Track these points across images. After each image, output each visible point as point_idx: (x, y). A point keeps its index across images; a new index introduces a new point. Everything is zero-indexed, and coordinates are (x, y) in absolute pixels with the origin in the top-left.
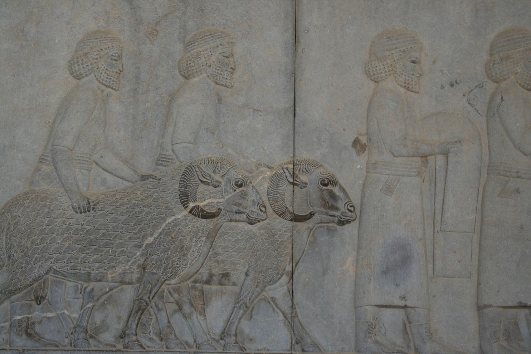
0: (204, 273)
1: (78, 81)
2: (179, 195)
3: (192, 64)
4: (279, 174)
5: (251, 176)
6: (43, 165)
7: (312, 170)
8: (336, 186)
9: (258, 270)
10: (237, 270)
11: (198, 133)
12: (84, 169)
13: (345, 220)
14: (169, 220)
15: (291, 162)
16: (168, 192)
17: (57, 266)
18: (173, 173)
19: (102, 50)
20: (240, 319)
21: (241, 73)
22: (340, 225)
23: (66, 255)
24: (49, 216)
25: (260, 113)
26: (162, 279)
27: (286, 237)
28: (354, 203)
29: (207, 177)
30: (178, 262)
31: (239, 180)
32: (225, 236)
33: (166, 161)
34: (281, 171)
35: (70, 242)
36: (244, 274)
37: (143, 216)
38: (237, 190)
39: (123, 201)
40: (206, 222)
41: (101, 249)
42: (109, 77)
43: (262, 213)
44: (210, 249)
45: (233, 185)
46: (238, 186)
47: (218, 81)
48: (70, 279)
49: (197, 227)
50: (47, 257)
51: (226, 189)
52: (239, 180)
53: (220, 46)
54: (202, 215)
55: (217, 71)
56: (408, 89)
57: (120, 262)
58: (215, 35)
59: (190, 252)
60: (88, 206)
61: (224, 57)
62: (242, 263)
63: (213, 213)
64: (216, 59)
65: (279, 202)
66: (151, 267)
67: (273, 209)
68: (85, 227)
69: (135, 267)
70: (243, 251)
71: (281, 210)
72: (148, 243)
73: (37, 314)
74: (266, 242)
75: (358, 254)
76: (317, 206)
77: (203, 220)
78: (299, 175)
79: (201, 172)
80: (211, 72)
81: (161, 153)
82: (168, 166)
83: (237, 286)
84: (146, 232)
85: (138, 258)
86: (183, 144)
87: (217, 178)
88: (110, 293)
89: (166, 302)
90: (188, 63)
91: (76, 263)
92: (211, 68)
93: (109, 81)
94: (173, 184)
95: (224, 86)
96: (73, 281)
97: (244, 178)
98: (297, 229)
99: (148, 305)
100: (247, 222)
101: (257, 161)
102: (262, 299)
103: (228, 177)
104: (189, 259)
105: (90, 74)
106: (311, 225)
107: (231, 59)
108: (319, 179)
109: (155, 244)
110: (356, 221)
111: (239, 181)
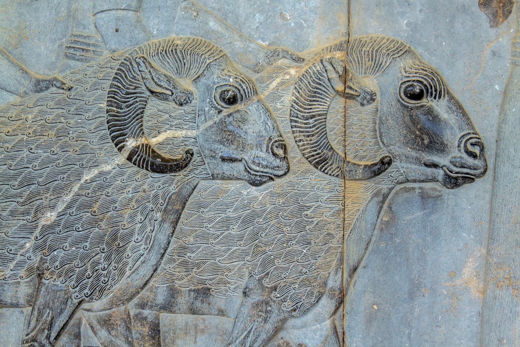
0: (158, 287)
2: (108, 123)
4: (314, 73)
5: (257, 80)
7: (386, 62)
8: (440, 97)
9: (269, 286)
10: (226, 283)
13: (459, 175)
14: (87, 177)
15: (341, 45)
16: (87, 115)
18: (96, 75)
26: (74, 299)
28: (481, 135)
29: (162, 84)
30: (104, 264)
31: (229, 88)
32: (202, 209)
33: (83, 50)
34: (318, 68)
36: (240, 292)
37: (37, 168)
38: (225, 110)
43: (278, 161)
44: (172, 236)
45: (215, 100)
46: (225, 102)
49: (144, 191)
51: (202, 110)
54: (153, 164)
59: (130, 244)
62: (236, 270)
63: (176, 160)
65: (313, 135)
66: (52, 273)
67: (301, 150)
70: (238, 243)
71: (318, 154)
74: (285, 225)
75: (488, 251)
76: (398, 145)
77: (156, 175)
79: (150, 72)
81: (75, 33)
82: (86, 60)
84: (41, 201)
94: (95, 100)
97: (240, 85)
104: (128, 257)
106: (385, 187)
108: (402, 84)
110: (486, 177)
111: (228, 91)
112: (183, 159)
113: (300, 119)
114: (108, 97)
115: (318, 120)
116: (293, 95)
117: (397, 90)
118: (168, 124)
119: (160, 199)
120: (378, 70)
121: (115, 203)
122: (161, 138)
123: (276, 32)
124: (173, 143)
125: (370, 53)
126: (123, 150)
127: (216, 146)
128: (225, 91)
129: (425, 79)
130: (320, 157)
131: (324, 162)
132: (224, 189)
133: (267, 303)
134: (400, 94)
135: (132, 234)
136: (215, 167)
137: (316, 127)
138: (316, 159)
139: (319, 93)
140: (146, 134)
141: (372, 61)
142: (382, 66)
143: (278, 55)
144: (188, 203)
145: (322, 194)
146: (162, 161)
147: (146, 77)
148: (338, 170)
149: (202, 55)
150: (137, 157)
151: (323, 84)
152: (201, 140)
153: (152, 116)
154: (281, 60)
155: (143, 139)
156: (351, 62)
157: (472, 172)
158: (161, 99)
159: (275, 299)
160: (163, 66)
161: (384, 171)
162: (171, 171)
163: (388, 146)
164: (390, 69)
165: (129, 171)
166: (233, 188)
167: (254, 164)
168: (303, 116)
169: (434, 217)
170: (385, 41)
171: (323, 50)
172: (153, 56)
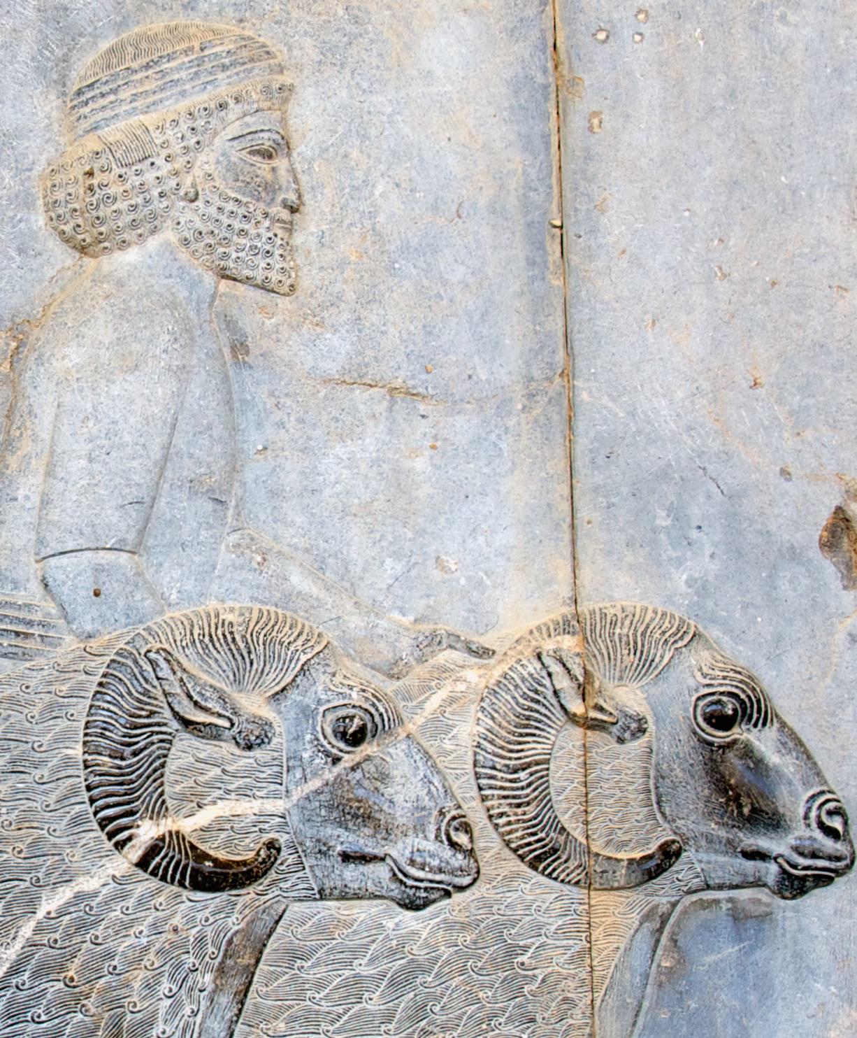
2: (89, 788)
3: (114, 189)
4: (523, 680)
5: (396, 692)
7: (662, 657)
8: (764, 724)
11: (154, 499)
15: (566, 622)
21: (324, 227)
22: (787, 894)
25: (422, 408)
29: (209, 705)
31: (352, 711)
38: (346, 757)
43: (460, 856)
45: (325, 737)
46: (347, 742)
49: (175, 930)
53: (231, 102)
54: (195, 872)
55: (226, 221)
61: (250, 153)
63: (244, 863)
64: (218, 162)
65: (528, 804)
67: (502, 835)
76: (692, 818)
77: (199, 895)
79: (181, 680)
80: (199, 225)
86: (89, 554)
87: (253, 704)
90: (95, 181)
92: (199, 203)
95: (257, 286)
97: (373, 705)
100: (393, 899)
103: (299, 698)
106: (664, 900)
107: (281, 163)
108: (698, 699)
111: (352, 718)
112: (260, 859)
113: (500, 771)
114: (86, 735)
115: (536, 772)
116: (478, 724)
117: (688, 712)
118: (220, 788)
119: (209, 945)
120: (647, 671)
121: (112, 958)
122: (204, 817)
123: (428, 596)
124: (232, 827)
125: (631, 638)
126: (129, 845)
127: (329, 831)
128: (344, 718)
129: (744, 691)
130: (544, 846)
131: (551, 855)
132: (344, 918)
134: (695, 718)
136: (326, 873)
137: (533, 787)
139: (536, 720)
140: (171, 812)
141: (635, 654)
142: (654, 665)
143: (440, 642)
144: (267, 951)
145: (545, 920)
146: (215, 866)
147: (173, 691)
148: (578, 871)
149: (289, 643)
150: (163, 859)
151: (542, 700)
152: (294, 820)
153: (184, 772)
154: (444, 653)
155: (170, 820)
156: (595, 656)
158: (203, 737)
160: (205, 667)
161: (665, 870)
162: (234, 887)
163: (674, 821)
164: (671, 669)
165: (139, 890)
166: (363, 916)
167: (413, 866)
168: (507, 766)
169: (759, 955)
170: (650, 615)
171: (531, 632)
172: (183, 648)
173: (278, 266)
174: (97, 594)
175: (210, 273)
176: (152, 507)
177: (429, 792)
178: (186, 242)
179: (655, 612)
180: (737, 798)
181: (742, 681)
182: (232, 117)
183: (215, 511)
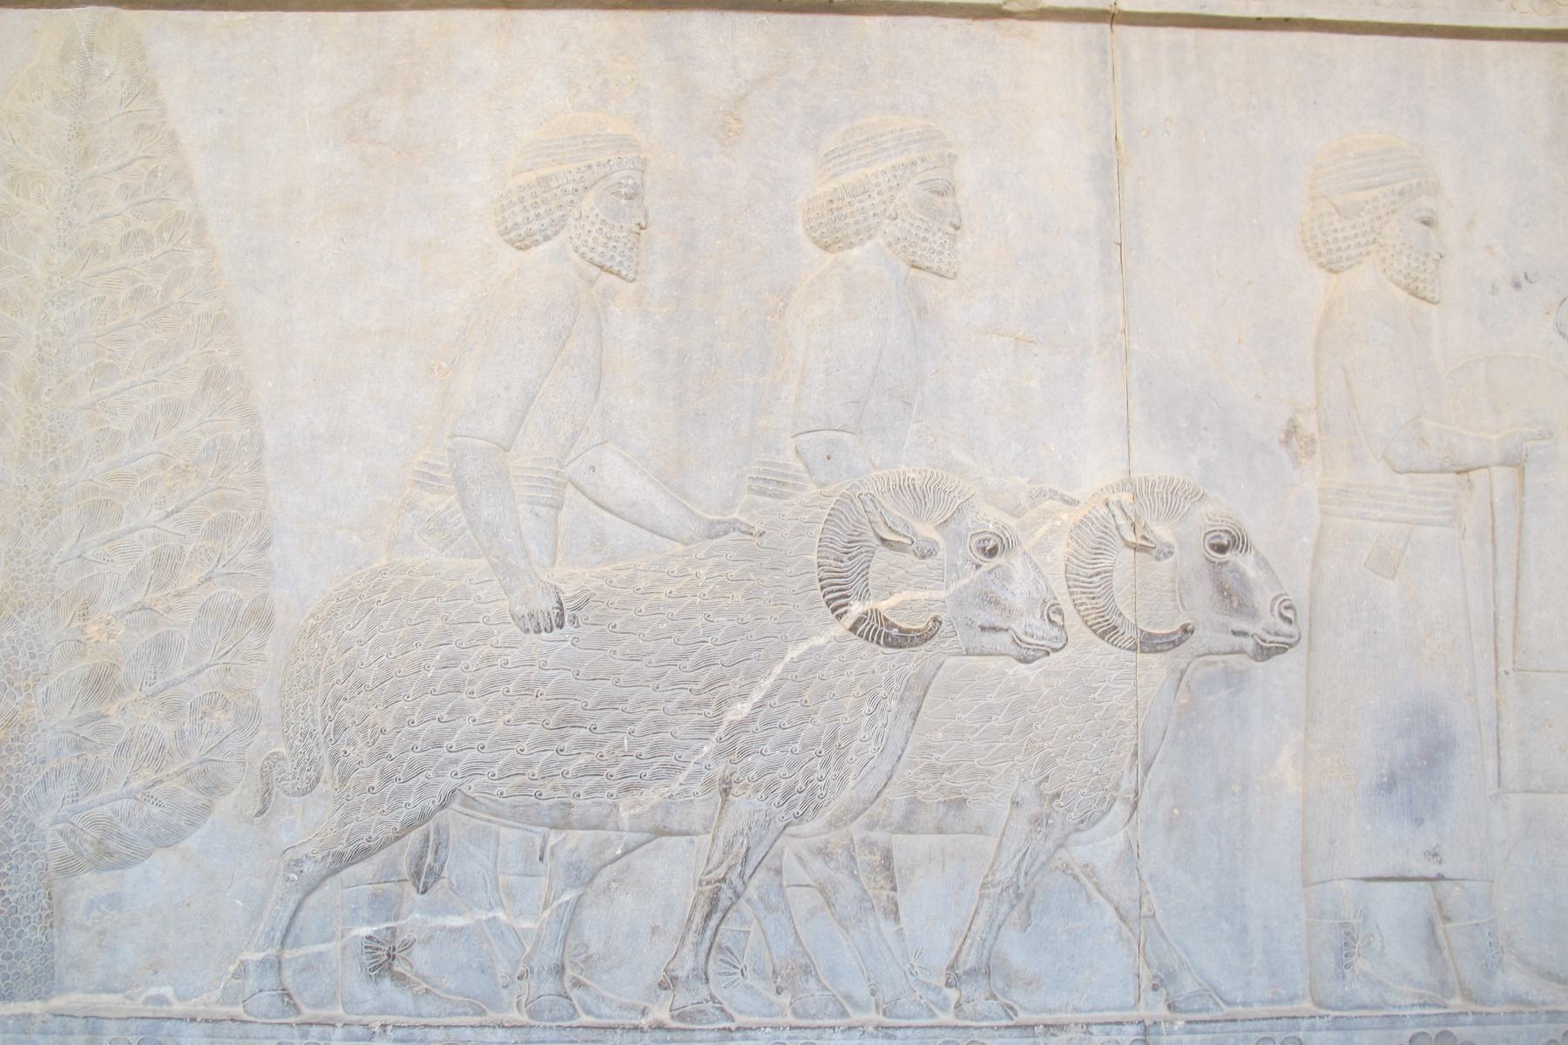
0: (893, 800)
1: (520, 253)
2: (820, 580)
3: (844, 211)
4: (1097, 519)
6: (423, 492)
7: (1184, 507)
8: (1246, 550)
11: (867, 401)
12: (543, 505)
13: (1273, 645)
14: (793, 653)
15: (1124, 484)
16: (788, 570)
17: (472, 784)
19: (590, 167)
20: (1000, 928)
23: (497, 754)
24: (444, 642)
27: (1119, 697)
28: (1291, 597)
30: (821, 773)
31: (990, 536)
33: (778, 482)
34: (1101, 512)
35: (508, 717)
38: (985, 564)
39: (657, 596)
40: (897, 657)
41: (600, 736)
42: (611, 244)
43: (1056, 630)
44: (911, 732)
45: (972, 552)
46: (985, 555)
47: (917, 258)
48: (510, 822)
49: (873, 672)
50: (442, 759)
52: (990, 536)
53: (919, 162)
54: (887, 635)
55: (914, 231)
56: (1414, 294)
57: (653, 774)
58: (905, 132)
59: (855, 744)
60: (556, 611)
61: (931, 192)
62: (1002, 773)
63: (919, 631)
65: (1099, 597)
66: (745, 787)
68: (548, 672)
69: (697, 787)
70: (1005, 738)
72: (735, 718)
73: (415, 917)
77: (889, 650)
78: (1148, 521)
83: (988, 835)
85: (706, 763)
86: (825, 433)
87: (926, 530)
88: (625, 860)
89: (788, 886)
90: (834, 206)
91: (527, 777)
92: (898, 221)
93: (611, 253)
96: (519, 828)
98: (1148, 673)
99: (738, 896)
100: (1013, 656)
101: (1029, 482)
102: (1056, 868)
103: (955, 527)
105: (556, 233)
107: (949, 200)
108: (1206, 534)
109: (754, 721)
111: (989, 540)
113: (1082, 576)
114: (819, 546)
122: (893, 601)
129: (1234, 530)
133: (1048, 816)
135: (854, 731)
137: (1103, 586)
138: (1102, 627)
139: (1105, 545)
140: (872, 597)
144: (931, 687)
146: (900, 632)
157: (1288, 641)
158: (894, 550)
159: (1057, 809)
166: (993, 666)
170: (1175, 482)
171: (1102, 490)
173: (947, 261)
174: (829, 458)
175: (905, 264)
176: (865, 405)
177: (1037, 588)
178: (890, 245)
179: (1179, 480)
180: (1230, 596)
181: (1233, 524)
182: (919, 170)
183: (905, 409)
